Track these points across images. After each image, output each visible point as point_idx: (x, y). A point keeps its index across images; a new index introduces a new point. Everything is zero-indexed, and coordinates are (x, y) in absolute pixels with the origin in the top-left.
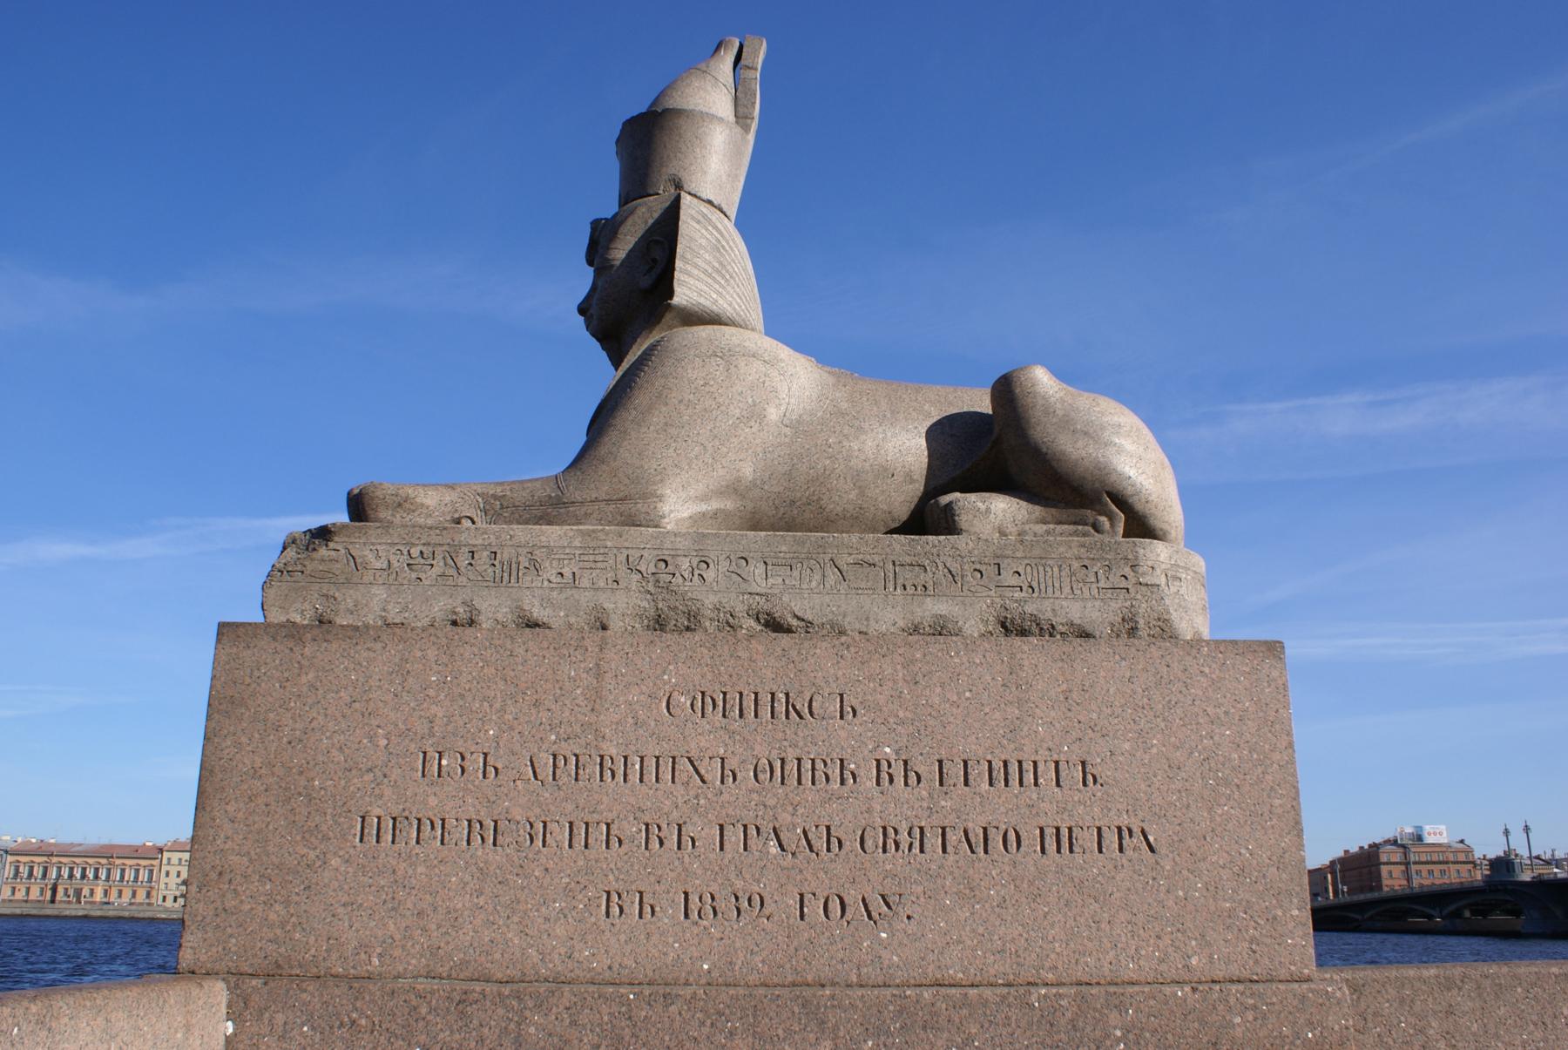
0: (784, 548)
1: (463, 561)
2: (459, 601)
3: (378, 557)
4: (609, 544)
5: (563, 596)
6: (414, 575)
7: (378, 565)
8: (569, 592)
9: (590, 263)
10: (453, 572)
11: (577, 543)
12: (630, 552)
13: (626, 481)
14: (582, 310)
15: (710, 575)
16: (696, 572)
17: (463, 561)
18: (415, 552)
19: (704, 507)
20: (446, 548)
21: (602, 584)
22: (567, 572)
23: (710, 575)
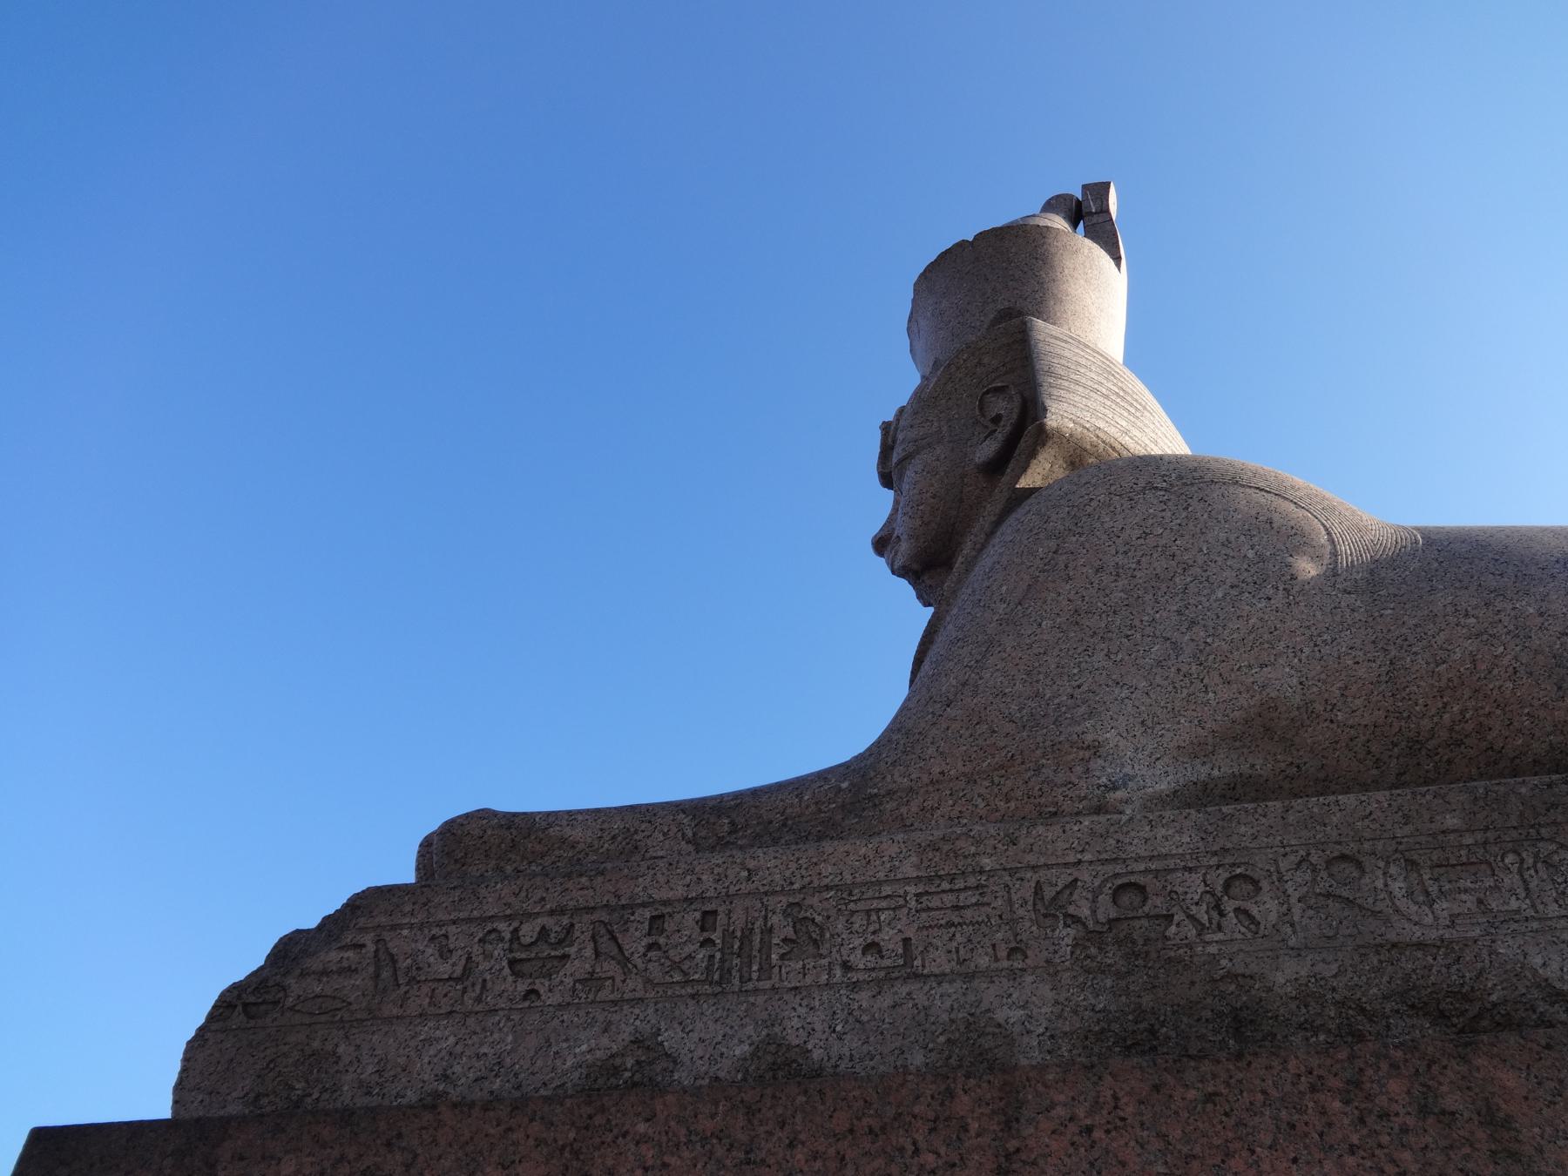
0: (1452, 821)
1: (635, 943)
2: (626, 1035)
3: (445, 953)
4: (987, 862)
5: (886, 1001)
6: (522, 987)
7: (444, 969)
8: (904, 990)
9: (887, 480)
10: (610, 968)
11: (908, 869)
12: (1042, 875)
13: (1010, 727)
14: (882, 544)
15: (1267, 908)
16: (1229, 906)
17: (635, 943)
18: (529, 932)
19: (1202, 772)
20: (595, 917)
21: (984, 961)
22: (889, 938)
23: (1267, 908)
